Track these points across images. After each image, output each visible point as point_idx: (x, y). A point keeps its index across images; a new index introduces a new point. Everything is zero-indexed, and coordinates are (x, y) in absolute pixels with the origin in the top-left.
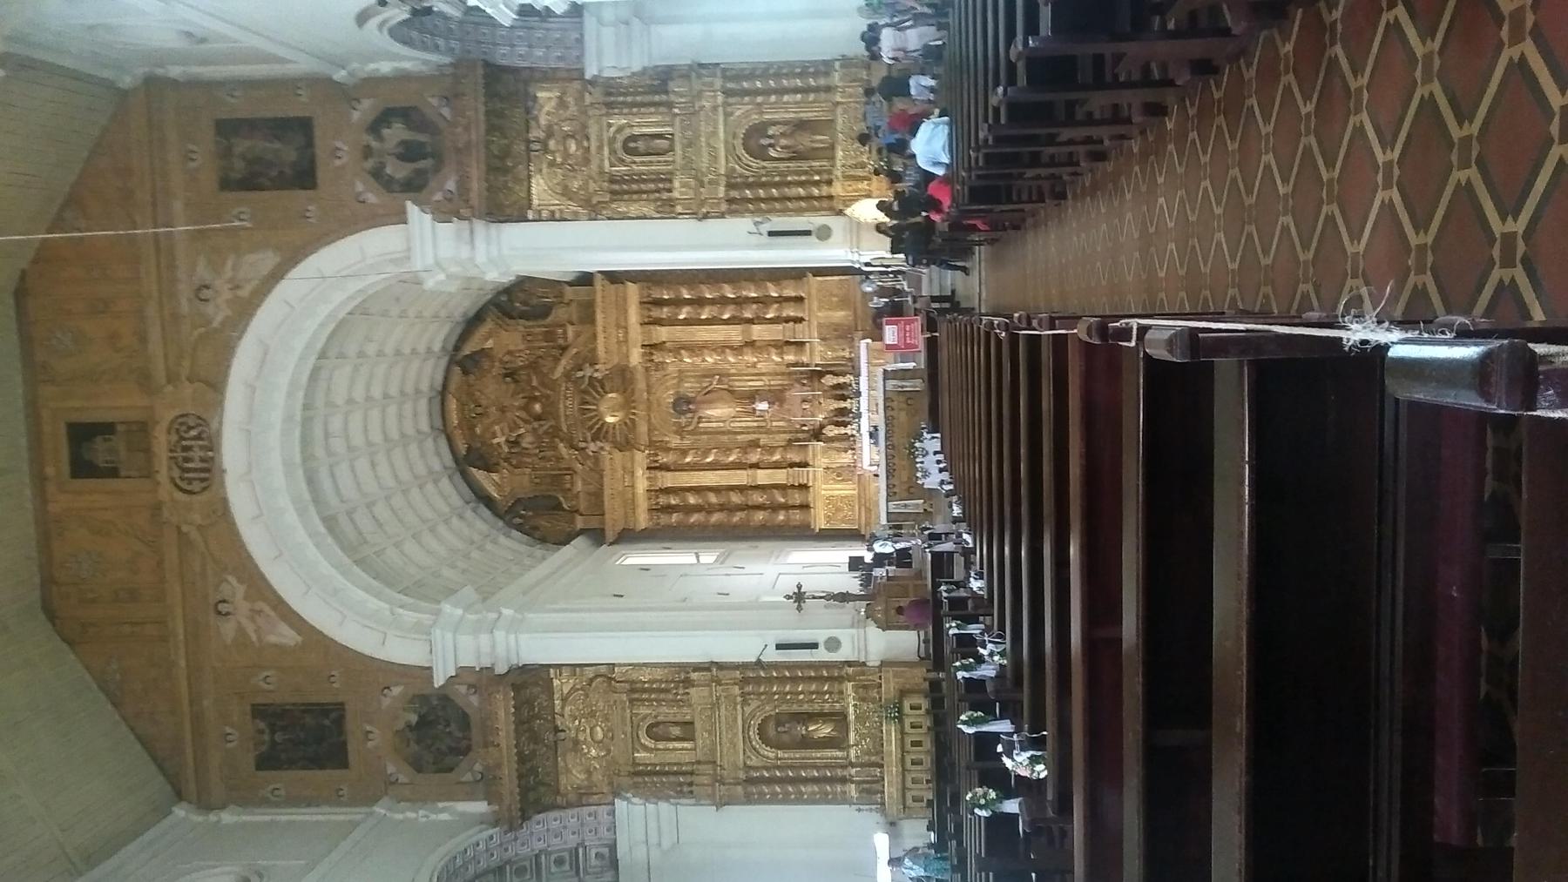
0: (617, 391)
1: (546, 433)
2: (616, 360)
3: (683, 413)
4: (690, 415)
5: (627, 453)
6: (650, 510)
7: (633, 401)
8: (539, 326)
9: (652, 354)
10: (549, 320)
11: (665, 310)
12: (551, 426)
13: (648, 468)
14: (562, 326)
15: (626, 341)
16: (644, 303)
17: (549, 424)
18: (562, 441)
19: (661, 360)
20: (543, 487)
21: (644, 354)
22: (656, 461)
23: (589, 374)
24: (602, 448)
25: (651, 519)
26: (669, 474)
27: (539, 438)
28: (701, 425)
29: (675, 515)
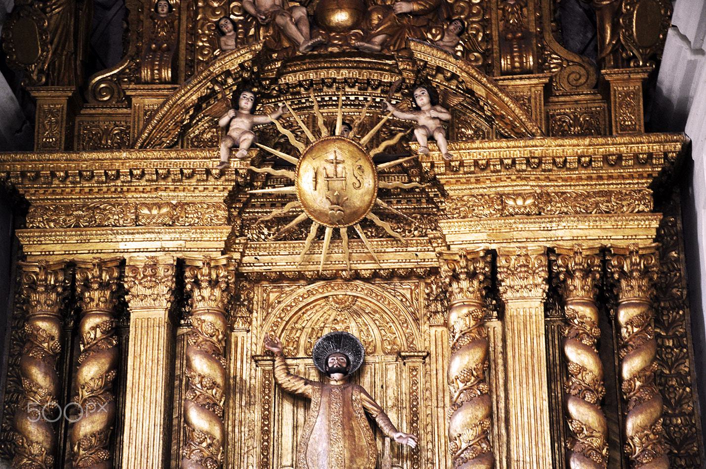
0: (383, 193)
1: (281, 32)
2: (452, 190)
3: (319, 357)
4: (314, 376)
5: (222, 213)
6: (71, 267)
7: (352, 233)
8: (539, 21)
9: (472, 276)
10: (557, 46)
11: (588, 313)
12: (295, 44)
13: (181, 265)
14: (540, 67)
15: (503, 213)
16: (605, 263)
17: (301, 39)
18: (261, 59)
19: (458, 298)
20: (147, 23)
21: (471, 257)
22: (197, 283)
23: (423, 119)
24: (235, 147)
25: (45, 268)
26: (160, 314)
27: (274, 15)
28: (288, 407)
29: (55, 332)
